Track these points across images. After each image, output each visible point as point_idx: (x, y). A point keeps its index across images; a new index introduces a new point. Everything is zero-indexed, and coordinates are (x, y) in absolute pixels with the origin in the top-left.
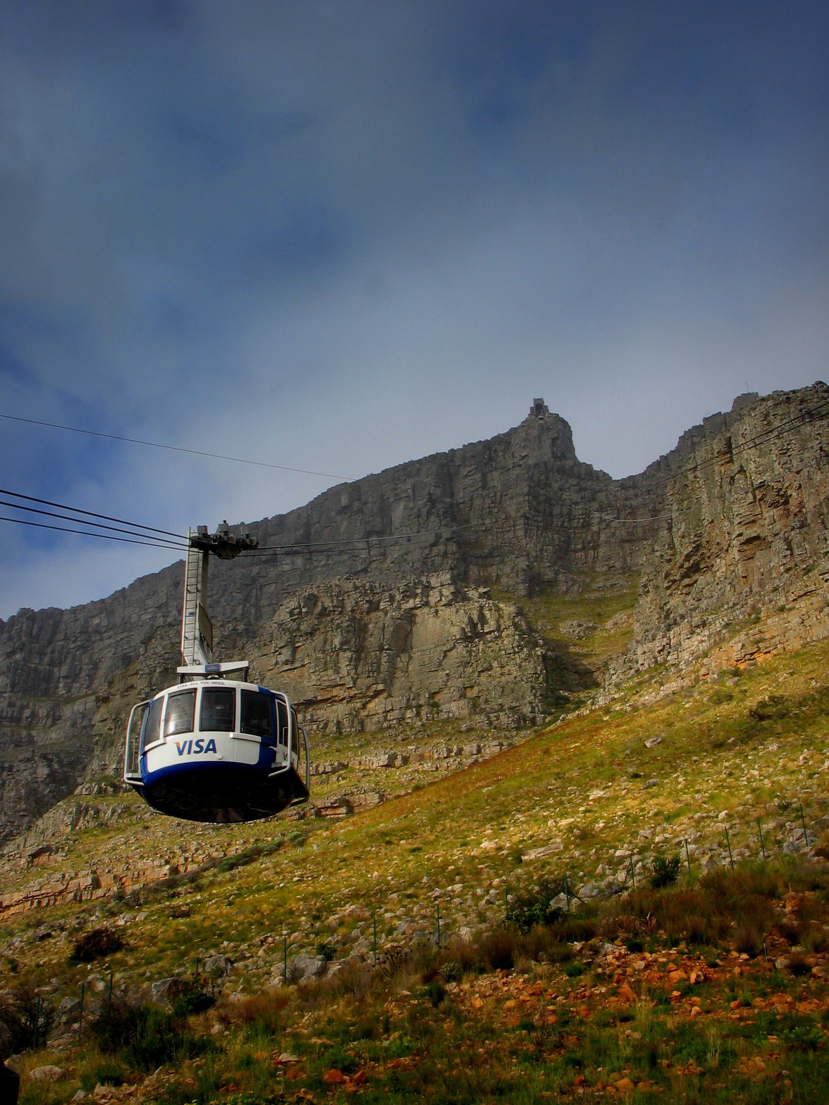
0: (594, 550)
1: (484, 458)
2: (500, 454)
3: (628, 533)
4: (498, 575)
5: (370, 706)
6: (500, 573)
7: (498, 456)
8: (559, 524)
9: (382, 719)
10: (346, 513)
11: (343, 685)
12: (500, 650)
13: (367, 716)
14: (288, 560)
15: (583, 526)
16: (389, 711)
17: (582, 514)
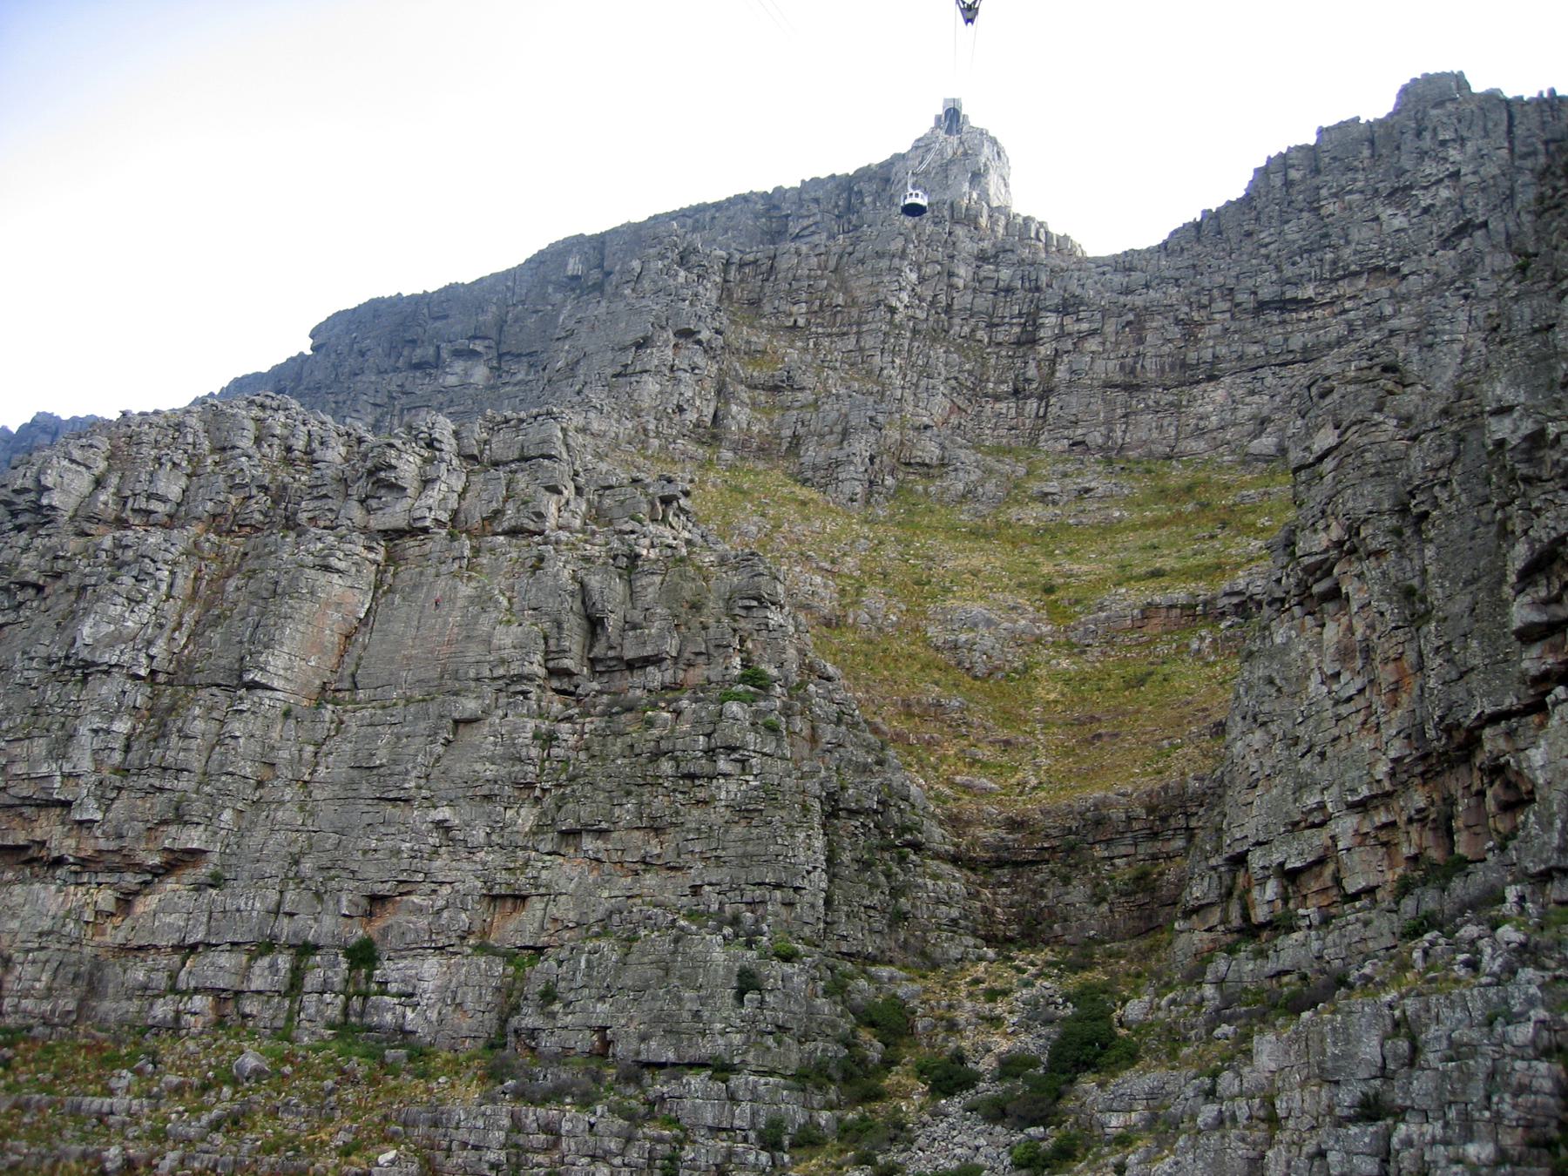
0: (1041, 398)
1: (837, 206)
2: (868, 200)
3: (1122, 366)
4: (795, 435)
5: (144, 905)
6: (801, 430)
7: (862, 203)
8: (966, 329)
9: (161, 980)
10: (573, 290)
11: (66, 804)
12: (656, 756)
13: (125, 950)
14: (459, 366)
15: (1019, 343)
16: (193, 948)
17: (1020, 315)
